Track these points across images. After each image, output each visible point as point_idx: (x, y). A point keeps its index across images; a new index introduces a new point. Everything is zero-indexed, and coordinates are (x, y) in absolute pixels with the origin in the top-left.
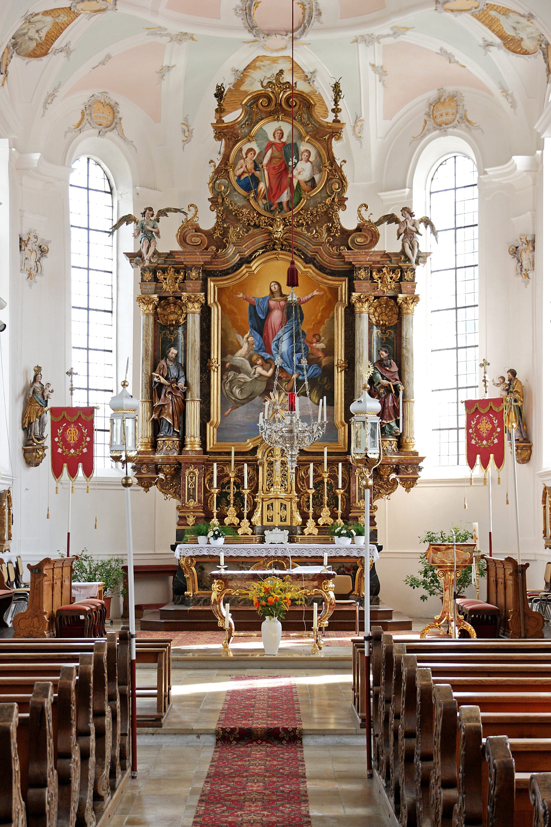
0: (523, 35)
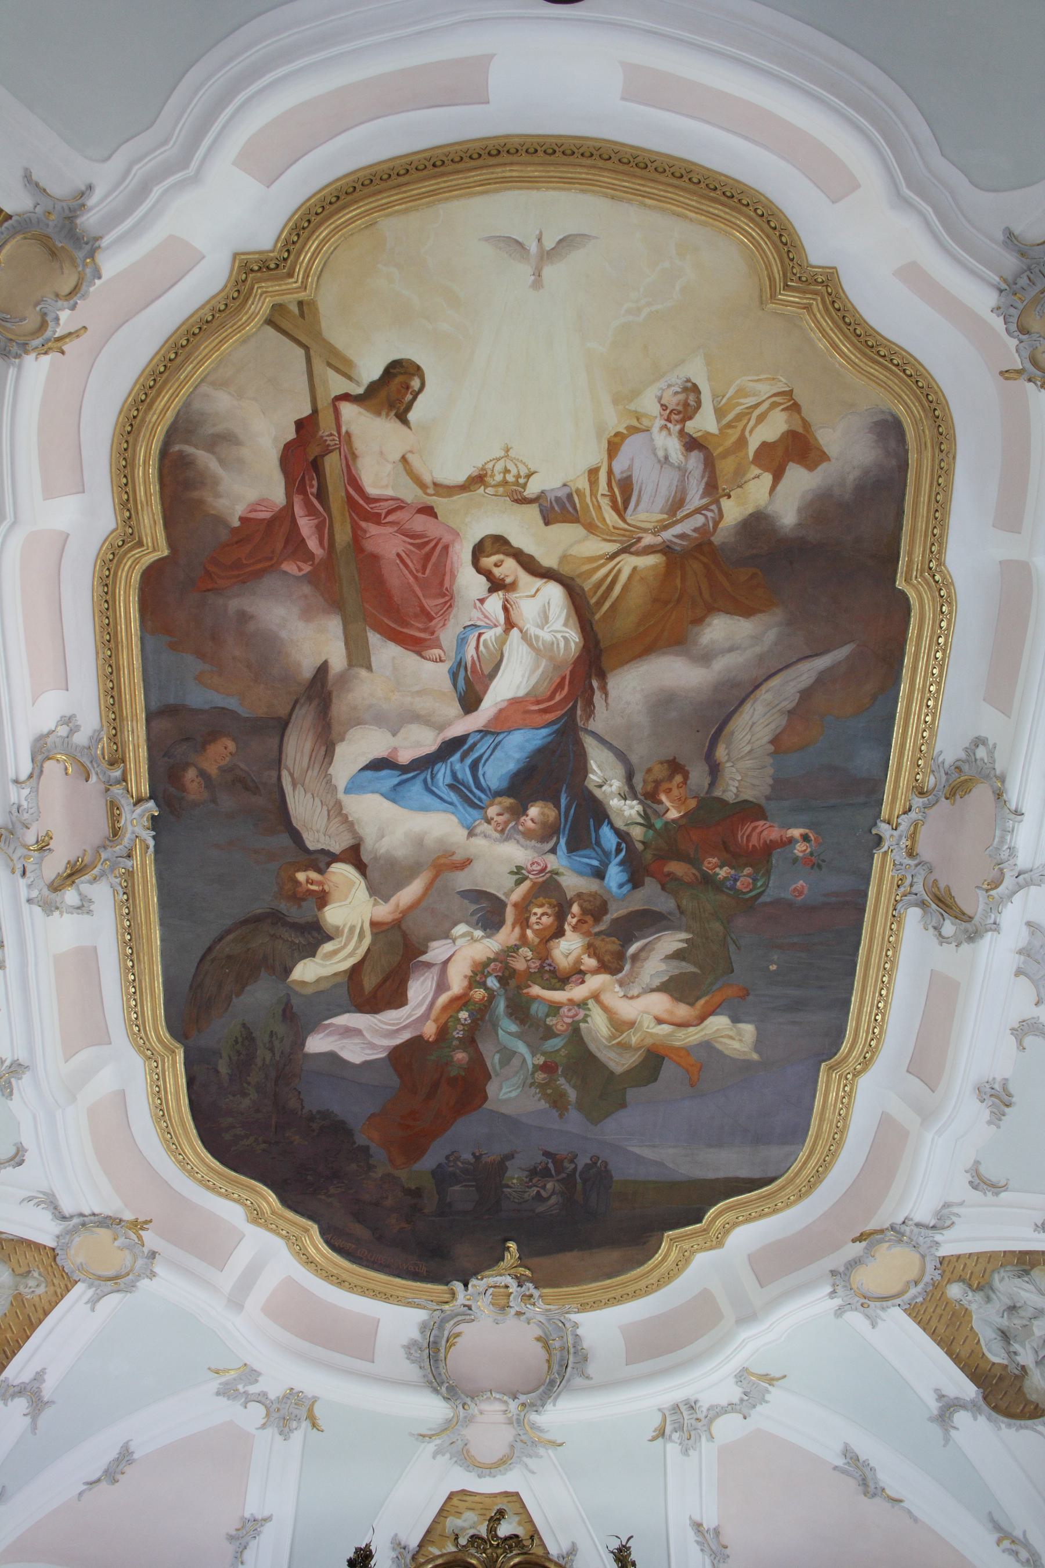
0: (1026, 1357)
